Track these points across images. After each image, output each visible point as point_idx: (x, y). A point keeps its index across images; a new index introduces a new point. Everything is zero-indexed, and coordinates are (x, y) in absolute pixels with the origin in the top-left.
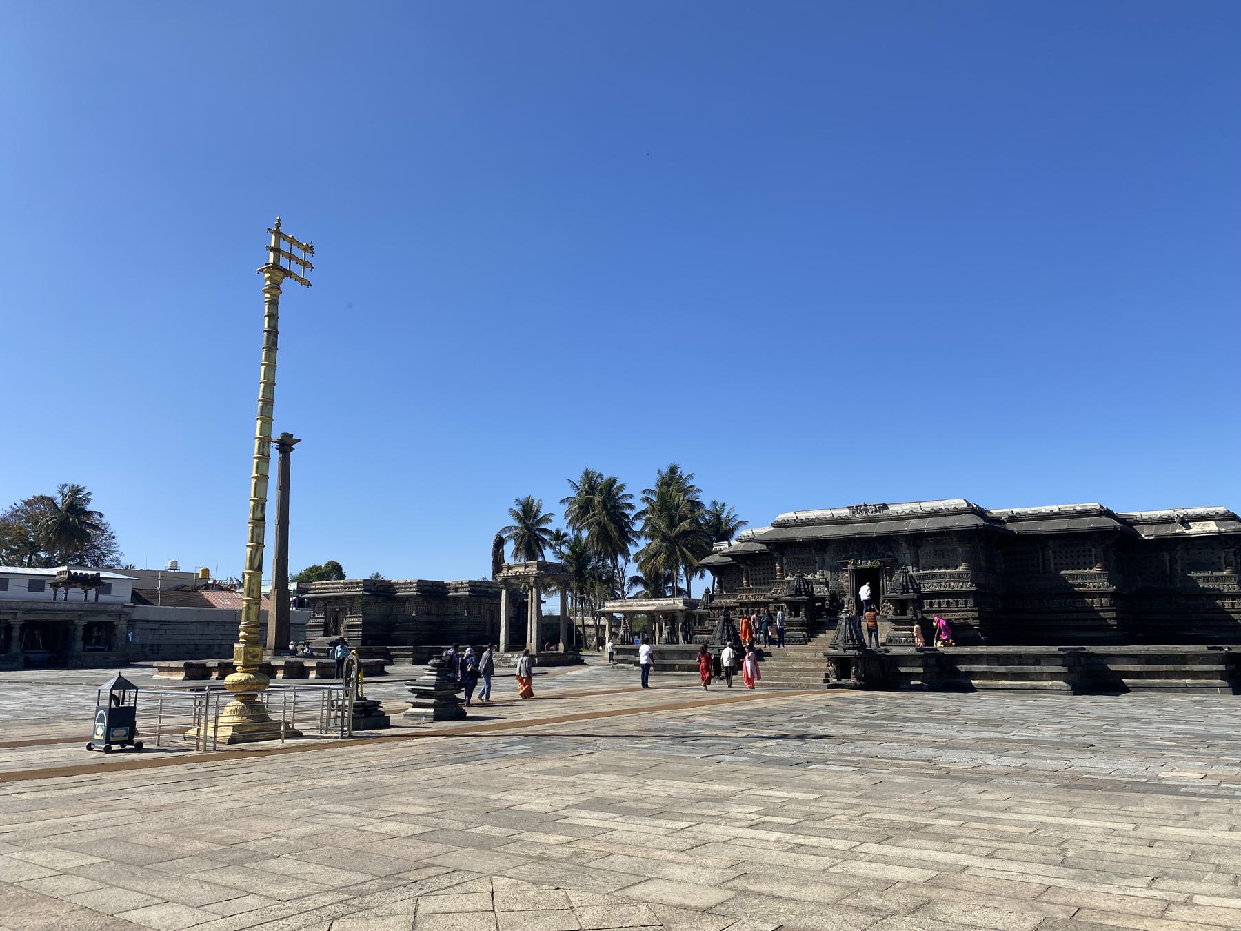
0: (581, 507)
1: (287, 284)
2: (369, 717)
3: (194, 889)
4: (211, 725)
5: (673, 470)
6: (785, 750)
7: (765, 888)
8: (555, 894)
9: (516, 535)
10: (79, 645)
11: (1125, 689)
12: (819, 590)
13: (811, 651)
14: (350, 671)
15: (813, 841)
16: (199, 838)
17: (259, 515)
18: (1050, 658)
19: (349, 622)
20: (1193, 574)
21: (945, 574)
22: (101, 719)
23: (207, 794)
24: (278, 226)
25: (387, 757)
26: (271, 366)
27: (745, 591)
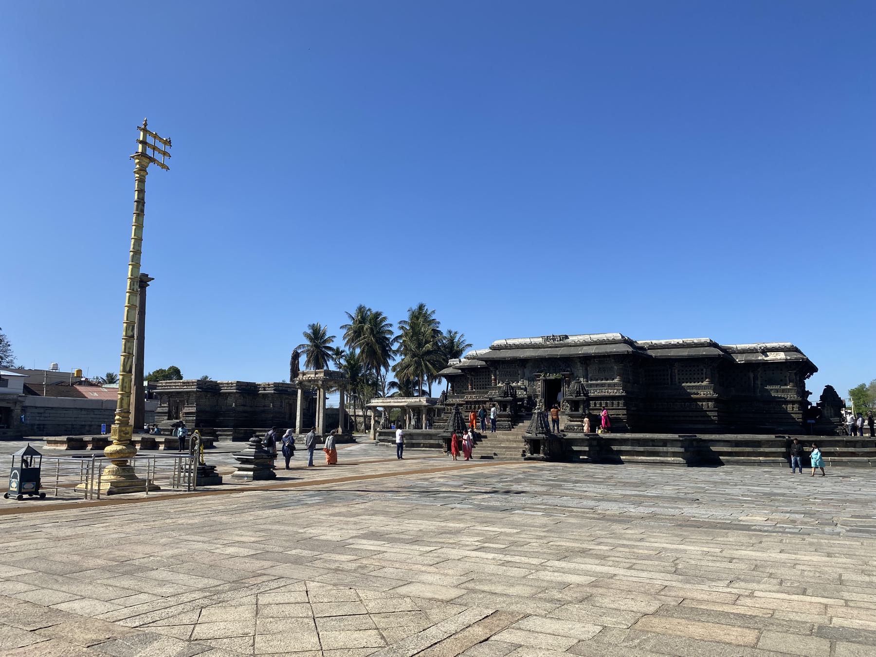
0: (355, 332)
1: (151, 168)
2: (207, 477)
3: (102, 589)
4: (95, 481)
6: (496, 501)
7: (486, 588)
8: (348, 592)
9: (308, 350)
11: (720, 463)
12: (520, 394)
13: (513, 434)
14: (194, 445)
15: (517, 559)
16: (99, 557)
18: (673, 442)
19: (186, 410)
20: (768, 387)
21: (605, 384)
22: (15, 477)
23: (98, 528)
24: (145, 125)
25: (223, 504)
26: (139, 227)
27: (469, 393)
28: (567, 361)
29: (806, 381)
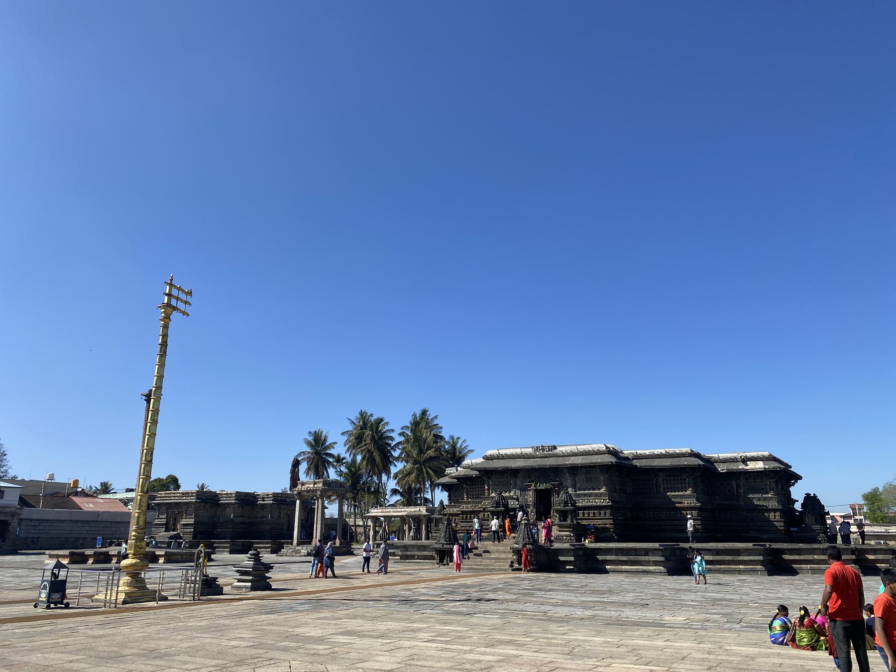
0: (356, 438)
1: (175, 315)
2: (210, 588)
5: (424, 413)
6: (463, 607)
7: (420, 663)
8: (319, 666)
9: (308, 458)
12: (512, 504)
13: (503, 545)
14: (199, 558)
15: (454, 647)
17: (149, 459)
20: (751, 496)
22: (45, 588)
23: (124, 629)
24: (171, 280)
26: (162, 365)
27: (465, 503)
29: (791, 489)
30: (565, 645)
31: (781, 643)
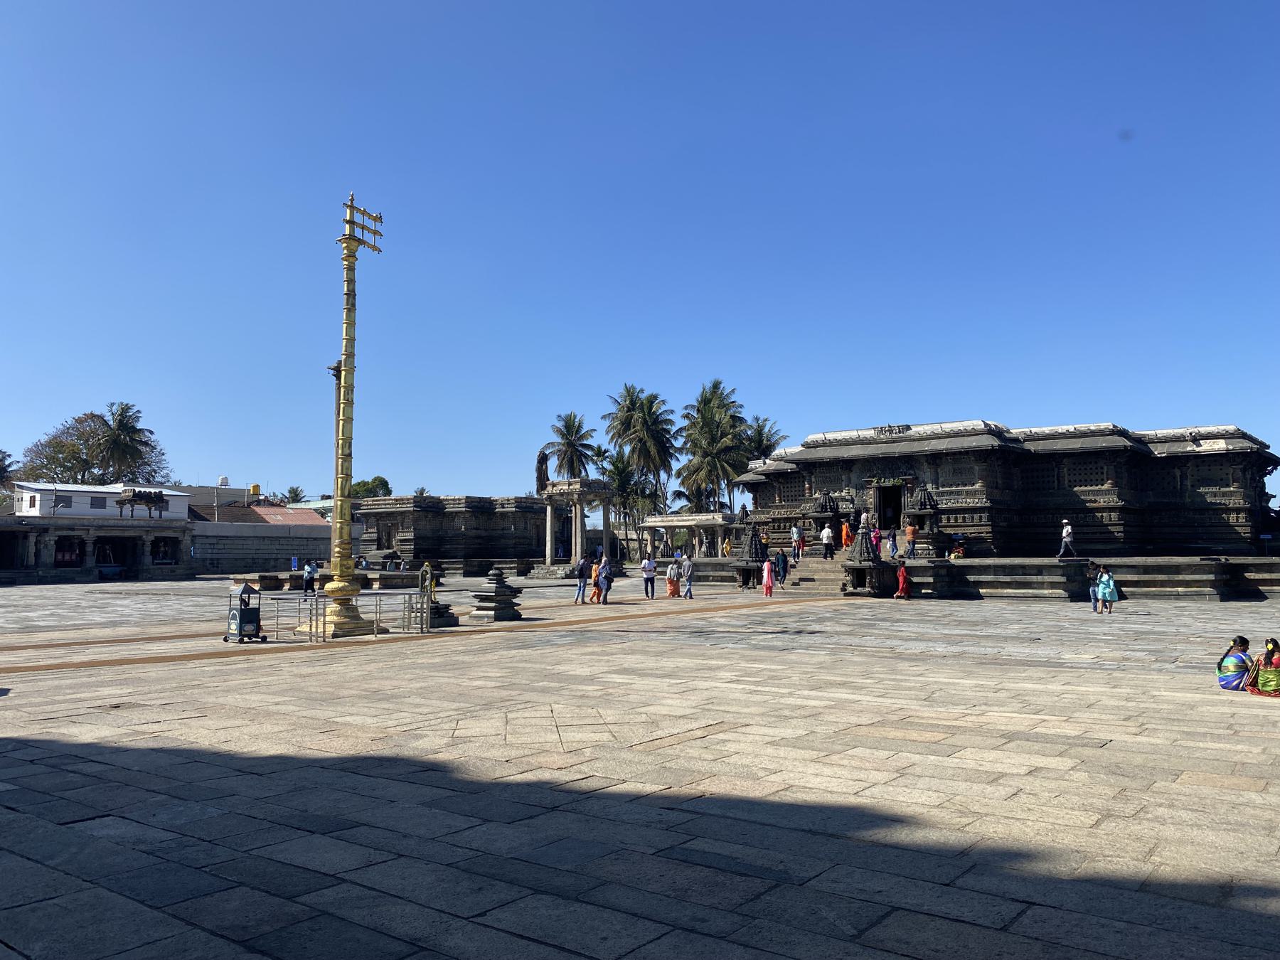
0: (622, 424)
1: (362, 251)
2: (442, 618)
5: (716, 386)
6: (779, 641)
7: (722, 708)
8: (590, 710)
10: (148, 559)
12: (844, 507)
14: (424, 580)
15: (767, 689)
17: (347, 452)
18: (1050, 569)
19: (400, 536)
20: (1202, 490)
22: (234, 617)
24: (352, 200)
27: (777, 507)
28: (908, 462)
30: (922, 688)
31: (1236, 688)
